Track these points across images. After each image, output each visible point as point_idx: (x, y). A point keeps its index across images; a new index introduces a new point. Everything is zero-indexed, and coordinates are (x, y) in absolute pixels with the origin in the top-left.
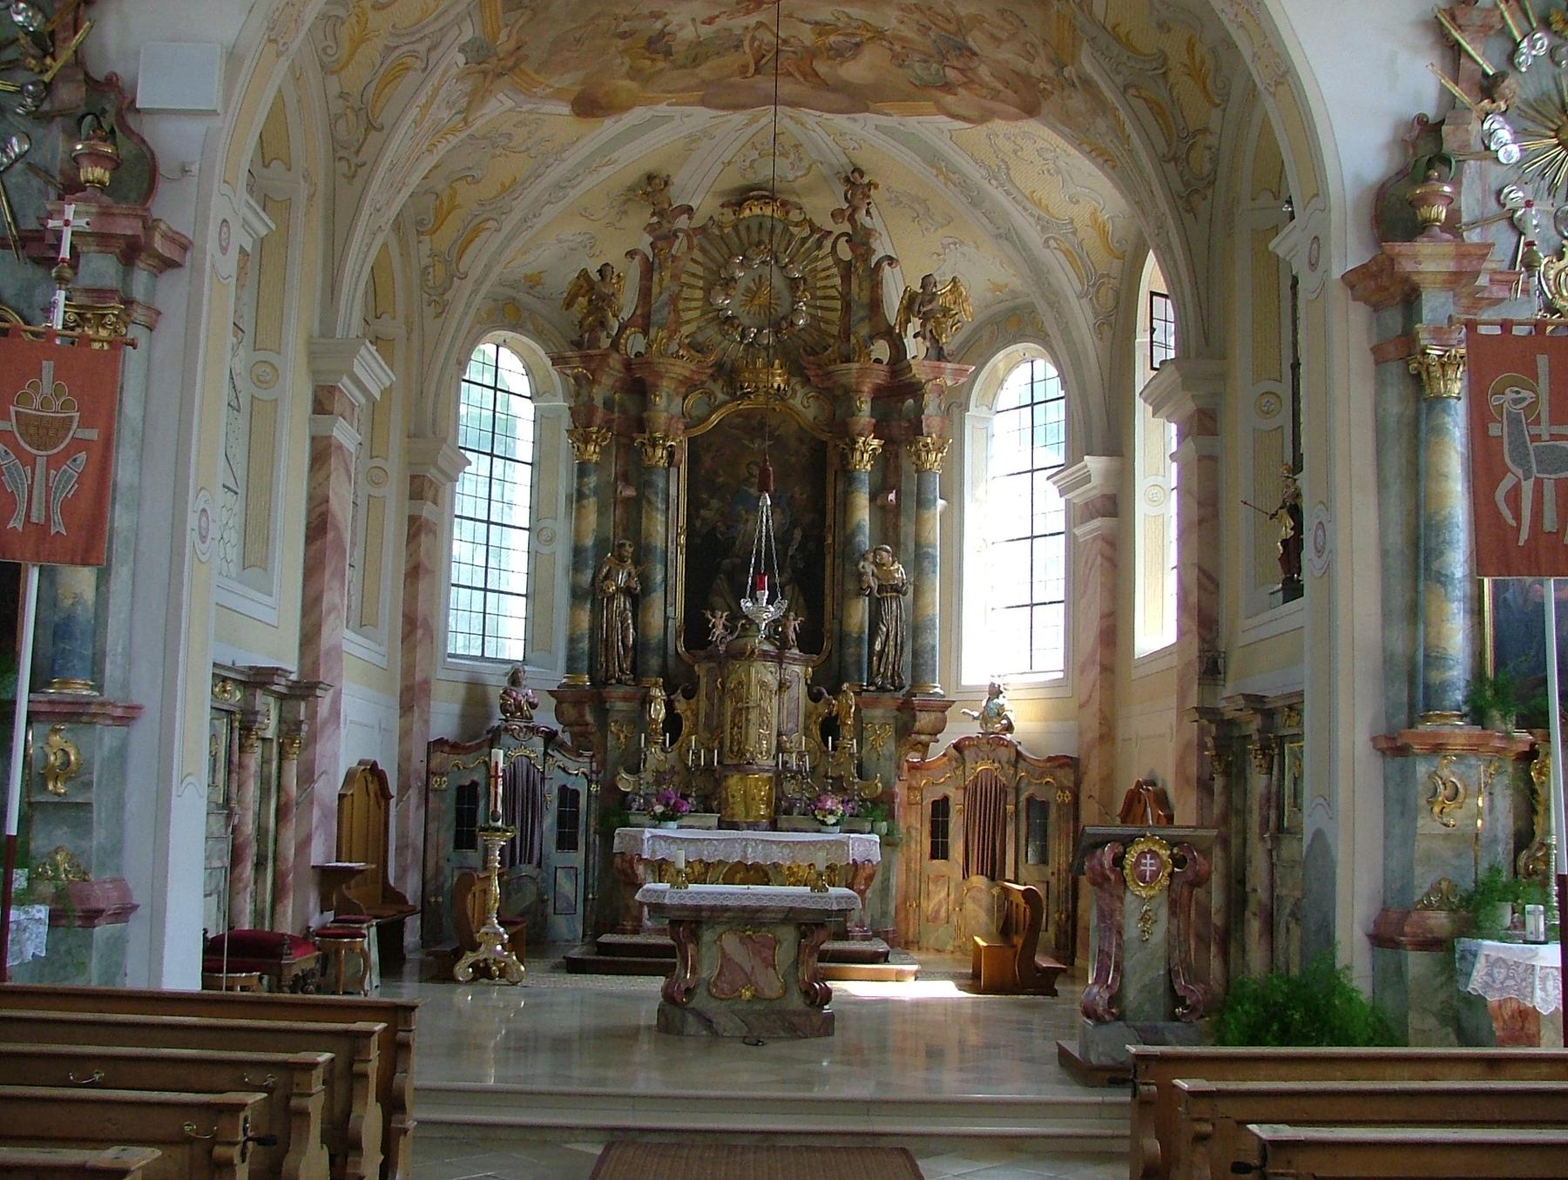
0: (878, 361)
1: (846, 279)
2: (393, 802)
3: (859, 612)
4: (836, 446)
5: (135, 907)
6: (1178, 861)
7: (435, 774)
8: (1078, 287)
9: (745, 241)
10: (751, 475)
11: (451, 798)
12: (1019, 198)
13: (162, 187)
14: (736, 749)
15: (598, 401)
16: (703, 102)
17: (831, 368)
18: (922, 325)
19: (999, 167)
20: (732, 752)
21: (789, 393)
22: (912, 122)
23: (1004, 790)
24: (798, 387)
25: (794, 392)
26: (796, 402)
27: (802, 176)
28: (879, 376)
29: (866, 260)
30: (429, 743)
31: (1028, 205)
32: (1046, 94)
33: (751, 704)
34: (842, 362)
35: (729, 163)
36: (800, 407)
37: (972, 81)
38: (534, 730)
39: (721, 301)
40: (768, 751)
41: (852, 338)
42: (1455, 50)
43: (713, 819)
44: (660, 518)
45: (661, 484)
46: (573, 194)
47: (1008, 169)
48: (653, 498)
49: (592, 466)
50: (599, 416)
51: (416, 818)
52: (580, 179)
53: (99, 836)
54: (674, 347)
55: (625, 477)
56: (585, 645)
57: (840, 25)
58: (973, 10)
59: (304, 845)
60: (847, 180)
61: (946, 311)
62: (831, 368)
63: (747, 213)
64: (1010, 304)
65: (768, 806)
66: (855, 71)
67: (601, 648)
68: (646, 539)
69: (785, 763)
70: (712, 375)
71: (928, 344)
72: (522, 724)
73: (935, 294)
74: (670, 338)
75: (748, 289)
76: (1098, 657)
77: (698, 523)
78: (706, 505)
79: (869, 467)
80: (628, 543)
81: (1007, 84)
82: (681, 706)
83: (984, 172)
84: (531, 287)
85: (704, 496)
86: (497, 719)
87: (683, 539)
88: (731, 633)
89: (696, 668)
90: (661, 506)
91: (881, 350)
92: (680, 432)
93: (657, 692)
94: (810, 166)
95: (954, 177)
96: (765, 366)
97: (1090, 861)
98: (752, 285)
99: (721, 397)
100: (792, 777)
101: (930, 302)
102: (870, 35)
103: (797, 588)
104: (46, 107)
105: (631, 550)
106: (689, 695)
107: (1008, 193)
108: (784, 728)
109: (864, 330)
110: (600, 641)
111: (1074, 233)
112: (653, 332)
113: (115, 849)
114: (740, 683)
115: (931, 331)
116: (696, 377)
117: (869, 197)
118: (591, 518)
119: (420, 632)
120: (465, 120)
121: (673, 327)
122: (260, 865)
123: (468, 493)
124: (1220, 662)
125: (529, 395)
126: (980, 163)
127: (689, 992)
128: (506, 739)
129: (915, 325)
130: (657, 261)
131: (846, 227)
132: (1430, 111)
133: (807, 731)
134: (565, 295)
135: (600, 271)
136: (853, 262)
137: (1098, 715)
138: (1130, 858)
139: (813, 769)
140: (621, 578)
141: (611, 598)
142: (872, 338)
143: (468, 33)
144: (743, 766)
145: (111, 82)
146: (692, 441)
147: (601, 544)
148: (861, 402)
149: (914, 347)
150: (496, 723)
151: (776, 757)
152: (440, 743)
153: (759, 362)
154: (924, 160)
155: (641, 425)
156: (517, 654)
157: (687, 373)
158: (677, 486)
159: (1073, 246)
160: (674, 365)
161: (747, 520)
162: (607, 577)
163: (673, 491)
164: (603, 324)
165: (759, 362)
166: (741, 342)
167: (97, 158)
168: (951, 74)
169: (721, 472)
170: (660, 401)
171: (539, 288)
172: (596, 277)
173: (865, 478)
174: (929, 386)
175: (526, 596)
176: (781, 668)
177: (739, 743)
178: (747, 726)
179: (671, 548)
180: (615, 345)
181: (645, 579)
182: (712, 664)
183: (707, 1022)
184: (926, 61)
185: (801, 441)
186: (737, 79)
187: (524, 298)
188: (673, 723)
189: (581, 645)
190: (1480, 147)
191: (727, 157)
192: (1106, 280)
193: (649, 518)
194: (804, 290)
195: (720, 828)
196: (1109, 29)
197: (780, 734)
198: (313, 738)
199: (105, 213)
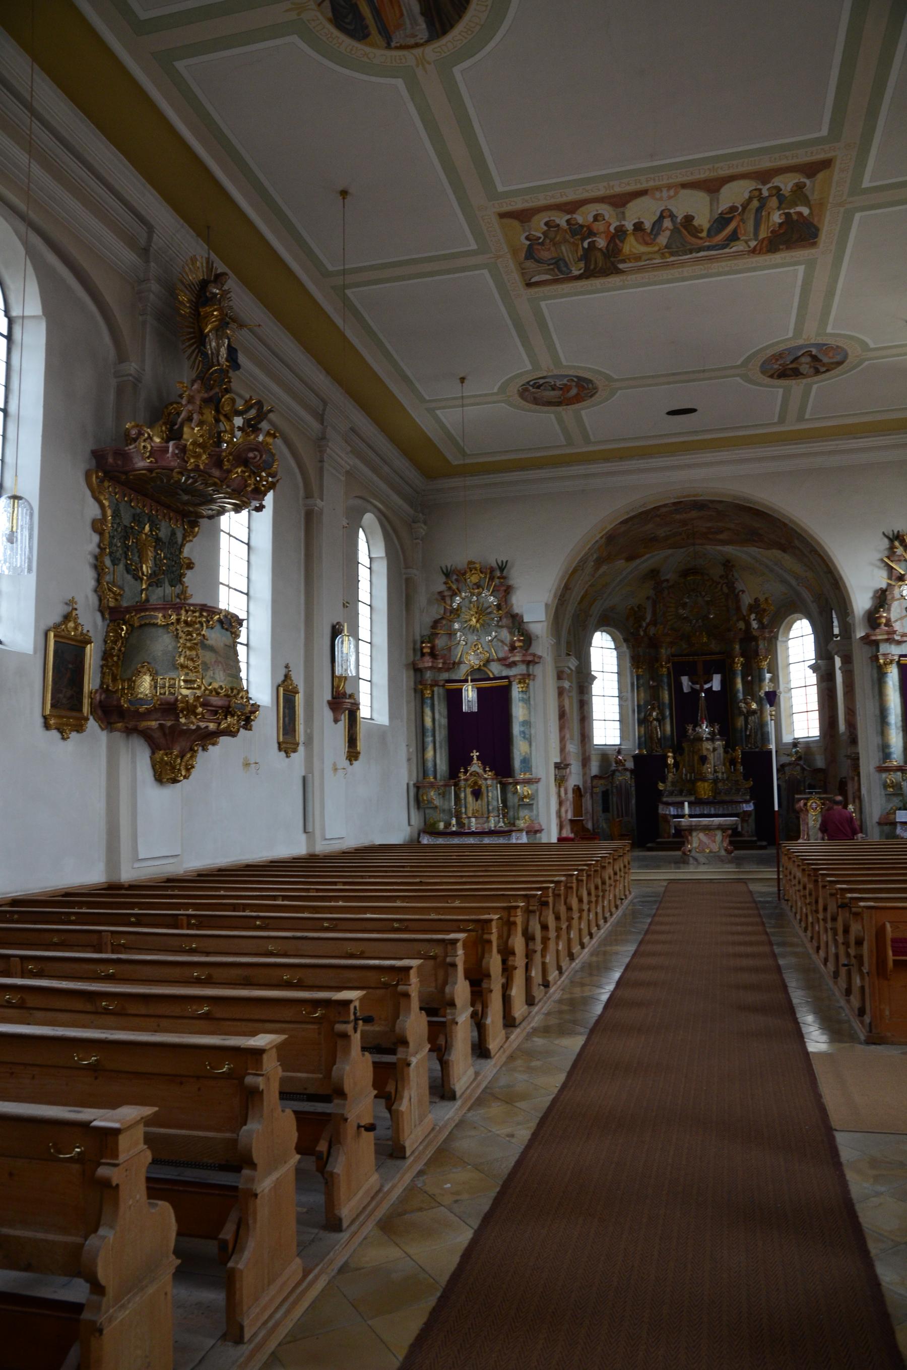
0: (741, 629)
3: (740, 722)
5: (543, 830)
6: (823, 804)
8: (812, 599)
11: (600, 795)
13: (533, 642)
22: (745, 549)
38: (626, 770)
39: (681, 611)
42: (890, 569)
51: (589, 803)
53: (535, 812)
55: (653, 679)
56: (643, 739)
59: (566, 812)
61: (764, 610)
66: (721, 537)
69: (717, 776)
82: (678, 759)
93: (670, 754)
104: (500, 624)
109: (735, 619)
113: (538, 815)
123: (597, 688)
127: (690, 851)
128: (617, 774)
129: (753, 616)
131: (726, 581)
132: (884, 586)
133: (724, 764)
135: (638, 607)
138: (809, 804)
139: (727, 778)
140: (654, 714)
141: (651, 722)
142: (738, 620)
145: (517, 614)
147: (647, 703)
149: (755, 625)
150: (613, 768)
152: (595, 777)
156: (617, 741)
164: (640, 626)
167: (519, 641)
170: (663, 651)
172: (636, 609)
173: (739, 673)
183: (696, 860)
188: (676, 764)
190: (899, 596)
197: (715, 766)
198: (567, 781)
199: (524, 655)
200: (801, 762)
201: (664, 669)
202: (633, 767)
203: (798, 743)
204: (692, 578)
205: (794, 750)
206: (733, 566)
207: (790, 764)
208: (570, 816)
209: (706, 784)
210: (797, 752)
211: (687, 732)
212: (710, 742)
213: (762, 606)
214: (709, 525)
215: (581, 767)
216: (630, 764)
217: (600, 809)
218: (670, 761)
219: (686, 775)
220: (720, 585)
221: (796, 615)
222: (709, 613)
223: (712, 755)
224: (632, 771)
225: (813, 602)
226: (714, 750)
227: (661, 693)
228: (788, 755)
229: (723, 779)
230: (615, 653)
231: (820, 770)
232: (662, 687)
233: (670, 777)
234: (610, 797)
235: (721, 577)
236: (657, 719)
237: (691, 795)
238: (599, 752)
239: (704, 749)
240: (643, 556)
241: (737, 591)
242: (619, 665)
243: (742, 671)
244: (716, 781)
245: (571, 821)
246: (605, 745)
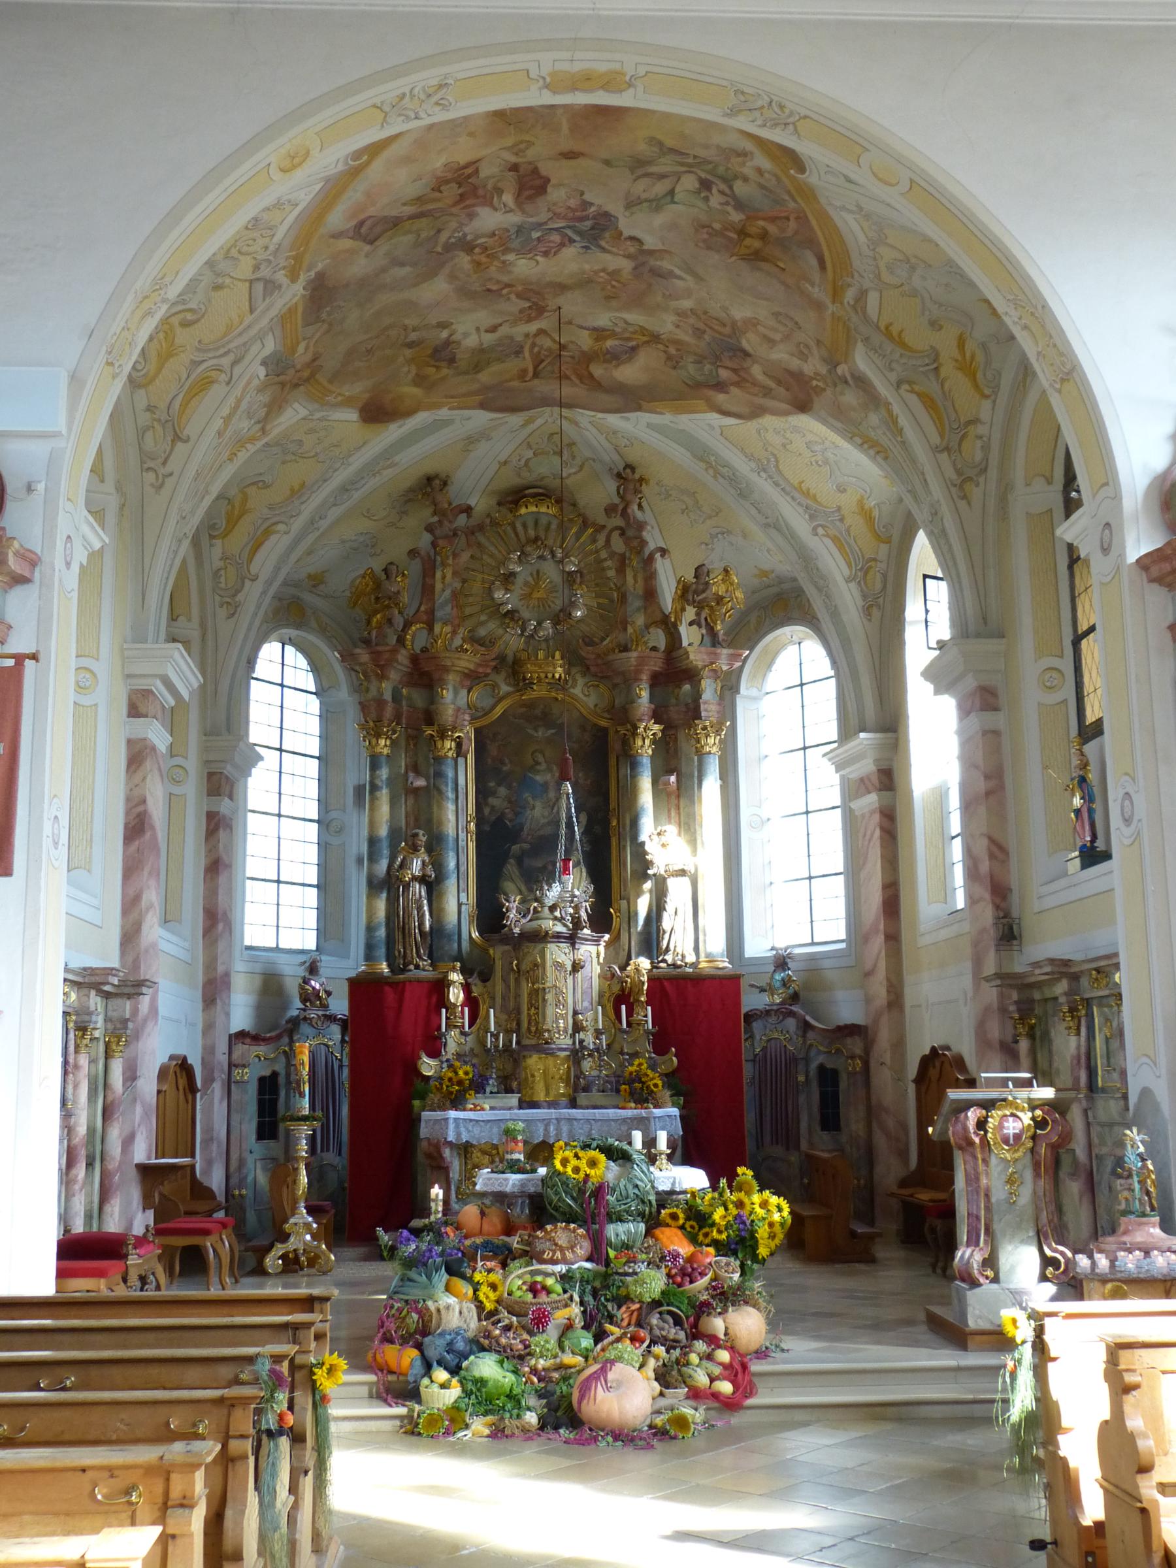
0: (654, 649)
1: (621, 570)
2: (198, 1095)
4: (617, 732)
7: (236, 1066)
8: (846, 572)
9: (523, 539)
10: (538, 763)
11: (253, 1090)
12: (788, 489)
14: (533, 1029)
15: (388, 696)
16: (483, 406)
17: (610, 657)
18: (698, 614)
19: (769, 461)
20: (529, 1030)
21: (570, 683)
22: (685, 421)
24: (578, 677)
25: (575, 681)
26: (577, 691)
27: (575, 473)
28: (656, 664)
29: (639, 552)
30: (230, 1036)
31: (797, 495)
32: (819, 391)
33: (548, 984)
34: (620, 651)
35: (505, 463)
36: (581, 695)
37: (745, 380)
38: (331, 1018)
39: (499, 595)
40: (565, 1031)
41: (629, 627)
43: (514, 1100)
44: (451, 807)
45: (450, 774)
46: (357, 495)
47: (777, 461)
48: (443, 788)
49: (383, 760)
50: (389, 712)
51: (220, 1109)
52: (363, 482)
54: (458, 642)
55: (416, 769)
56: (382, 933)
57: (617, 330)
58: (748, 314)
59: (128, 1141)
60: (619, 475)
61: (720, 600)
62: (610, 657)
63: (523, 511)
64: (775, 590)
65: (567, 1084)
66: (629, 373)
67: (398, 936)
68: (438, 827)
69: (581, 1041)
70: (495, 667)
71: (704, 631)
72: (320, 1013)
73: (707, 583)
74: (454, 633)
75: (526, 583)
76: (882, 927)
77: (487, 811)
78: (494, 793)
79: (650, 752)
80: (421, 832)
81: (779, 383)
83: (753, 465)
84: (314, 586)
85: (492, 784)
86: (296, 1007)
87: (472, 826)
88: (524, 916)
89: (491, 952)
90: (451, 795)
91: (659, 638)
92: (466, 723)
93: (455, 977)
94: (583, 464)
95: (724, 470)
96: (546, 658)
97: (954, 1127)
98: (530, 579)
99: (505, 688)
100: (590, 1055)
101: (703, 591)
102: (645, 339)
103: (584, 870)
105: (424, 839)
106: (485, 978)
107: (777, 484)
108: (579, 1008)
109: (640, 620)
110: (397, 926)
111: (842, 520)
112: (437, 628)
114: (536, 965)
115: (706, 619)
116: (481, 670)
117: (640, 492)
118: (384, 809)
119: (220, 926)
120: (263, 430)
121: (457, 622)
122: (90, 1165)
124: (1015, 927)
125: (314, 690)
126: (750, 457)
128: (305, 1028)
130: (438, 558)
131: (618, 521)
134: (348, 594)
135: (385, 570)
136: (627, 554)
137: (885, 982)
140: (416, 866)
141: (407, 886)
143: (270, 346)
144: (544, 1048)
146: (477, 731)
147: (395, 834)
148: (641, 689)
150: (295, 1013)
151: (573, 1036)
152: (241, 1035)
153: (541, 654)
154: (695, 456)
155: (429, 718)
157: (472, 667)
158: (465, 774)
159: (841, 533)
160: (459, 659)
161: (533, 808)
162: (402, 866)
163: (461, 781)
165: (541, 654)
166: (522, 634)
168: (724, 374)
169: (507, 761)
170: (447, 695)
171: (322, 587)
174: (706, 672)
175: (318, 886)
176: (574, 948)
177: (537, 1023)
178: (544, 1006)
179: (462, 835)
180: (401, 641)
181: (438, 865)
182: (507, 948)
184: (699, 362)
185: (583, 728)
186: (516, 383)
187: (308, 597)
189: (377, 934)
191: (502, 458)
192: (872, 563)
193: (440, 807)
194: (581, 583)
195: (520, 1108)
196: (883, 328)
197: (575, 1013)
198: (137, 1036)
201: (448, 744)
202: (347, 1013)
203: (790, 956)
204: (532, 509)
205: (778, 977)
206: (642, 480)
207: (768, 1013)
208: (142, 1152)
209: (550, 1061)
210: (785, 983)
211: (503, 916)
212: (565, 947)
213: (714, 589)
214: (603, 319)
215: (200, 1005)
216: (340, 1005)
217: (249, 1126)
218: (456, 995)
219: (496, 1036)
220: (606, 532)
221: (786, 631)
222: (573, 605)
223: (570, 980)
224: (344, 1024)
225: (848, 580)
226: (576, 967)
227: (435, 808)
228: (762, 990)
229: (597, 1050)
230: (314, 704)
231: (852, 1030)
232: (440, 792)
233: (453, 1042)
234: (282, 1093)
235: (610, 510)
236: (423, 880)
237: (509, 1090)
238: (258, 968)
239: (549, 963)
240: (409, 413)
241: (647, 552)
242: (325, 737)
243: (652, 757)
244: (577, 1054)
245: (146, 1172)
246: (277, 949)
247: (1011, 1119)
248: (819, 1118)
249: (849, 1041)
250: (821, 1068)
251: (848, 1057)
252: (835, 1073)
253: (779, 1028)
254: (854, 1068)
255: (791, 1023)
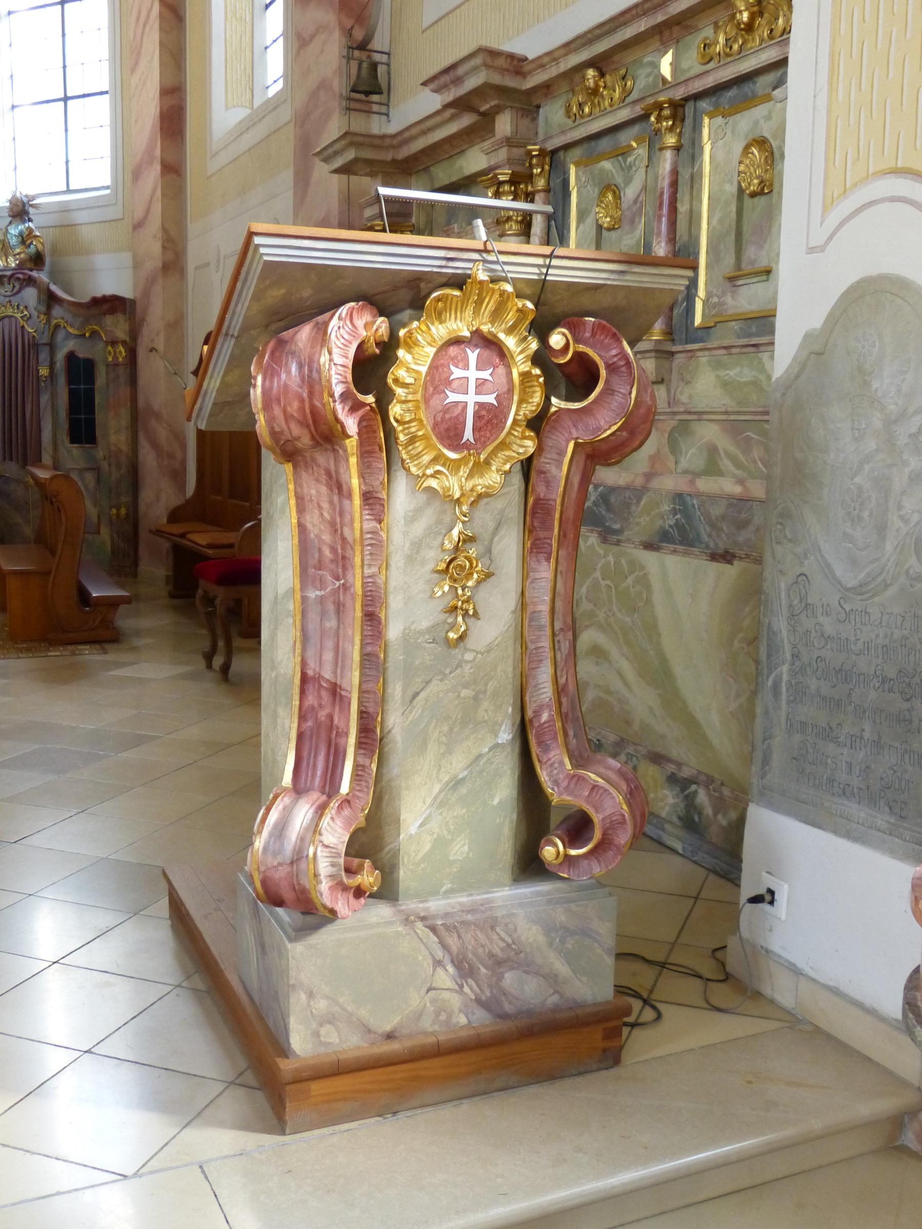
23: (35, 346)
76: (158, 152)
124: (381, 69)
137: (160, 235)
200: (42, 276)
205: (14, 231)
210: (25, 239)
247: (473, 356)
248: (67, 427)
249: (109, 320)
250: (71, 357)
251: (107, 343)
252: (90, 365)
253: (15, 300)
254: (115, 357)
255: (30, 295)
